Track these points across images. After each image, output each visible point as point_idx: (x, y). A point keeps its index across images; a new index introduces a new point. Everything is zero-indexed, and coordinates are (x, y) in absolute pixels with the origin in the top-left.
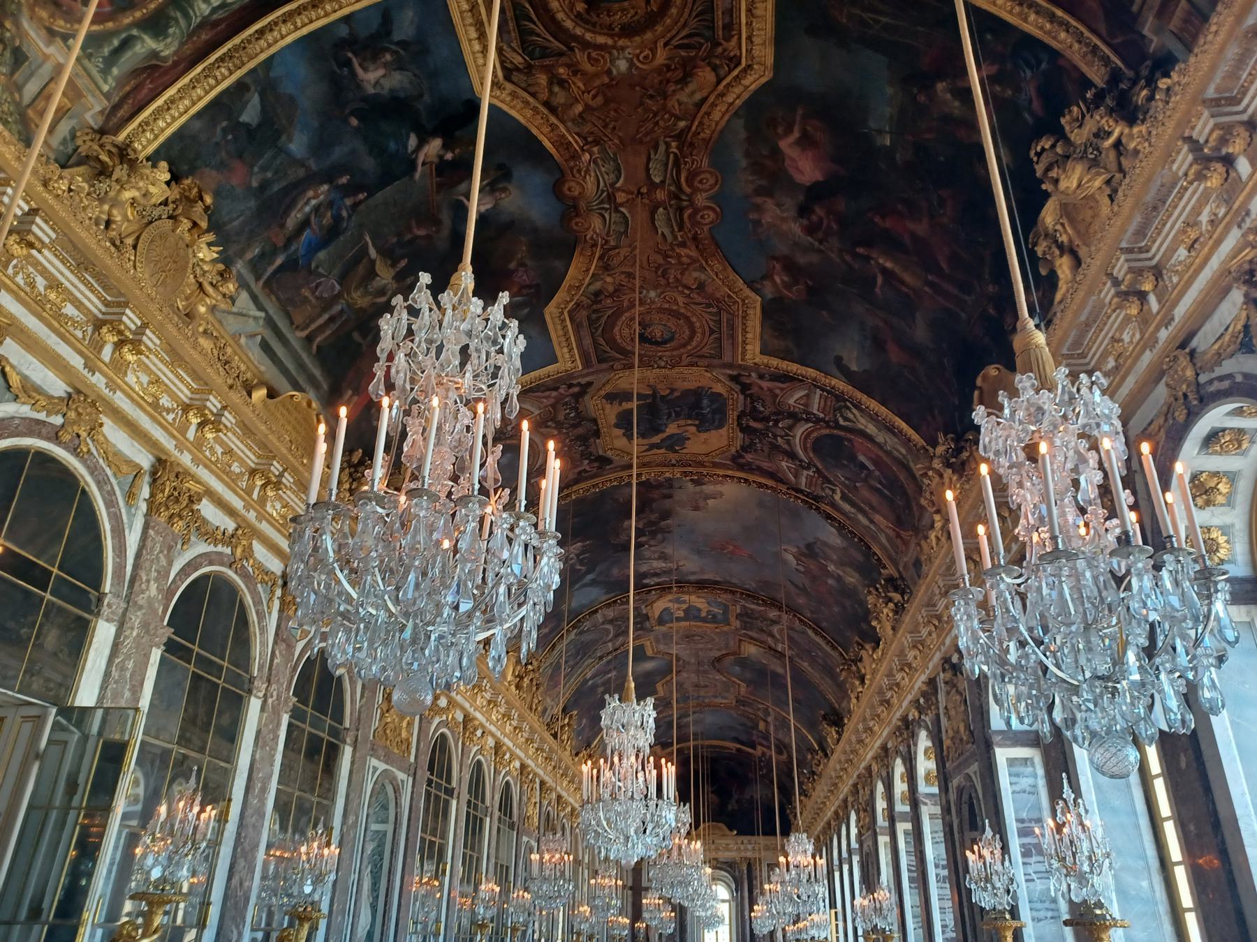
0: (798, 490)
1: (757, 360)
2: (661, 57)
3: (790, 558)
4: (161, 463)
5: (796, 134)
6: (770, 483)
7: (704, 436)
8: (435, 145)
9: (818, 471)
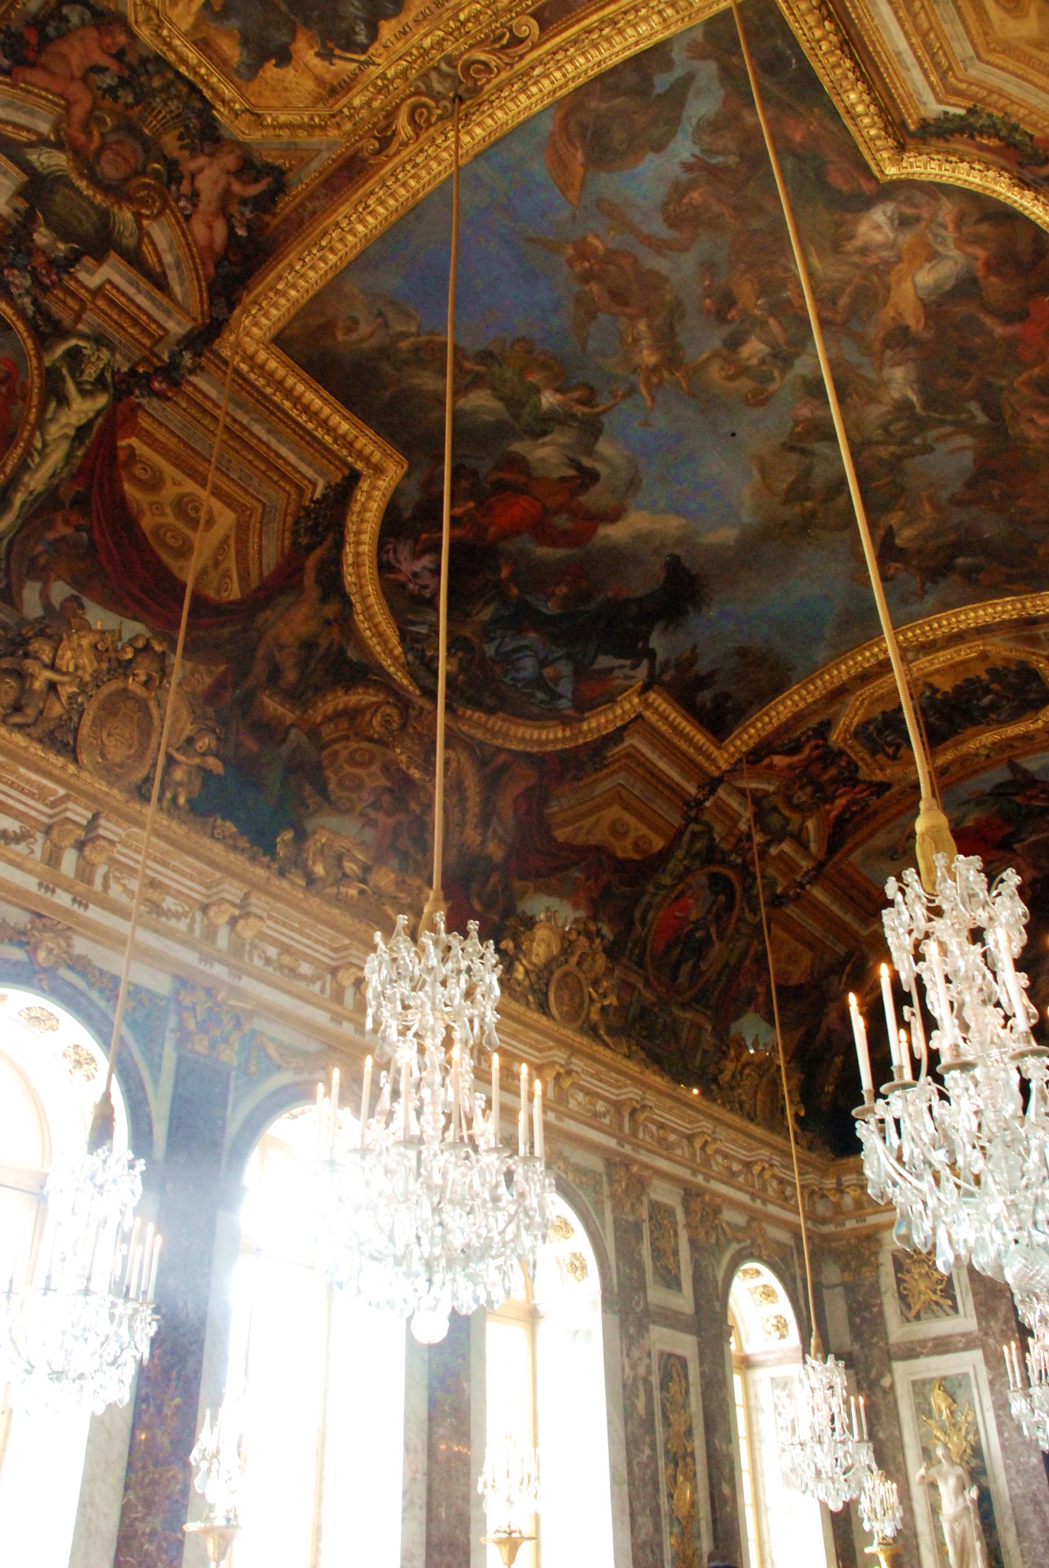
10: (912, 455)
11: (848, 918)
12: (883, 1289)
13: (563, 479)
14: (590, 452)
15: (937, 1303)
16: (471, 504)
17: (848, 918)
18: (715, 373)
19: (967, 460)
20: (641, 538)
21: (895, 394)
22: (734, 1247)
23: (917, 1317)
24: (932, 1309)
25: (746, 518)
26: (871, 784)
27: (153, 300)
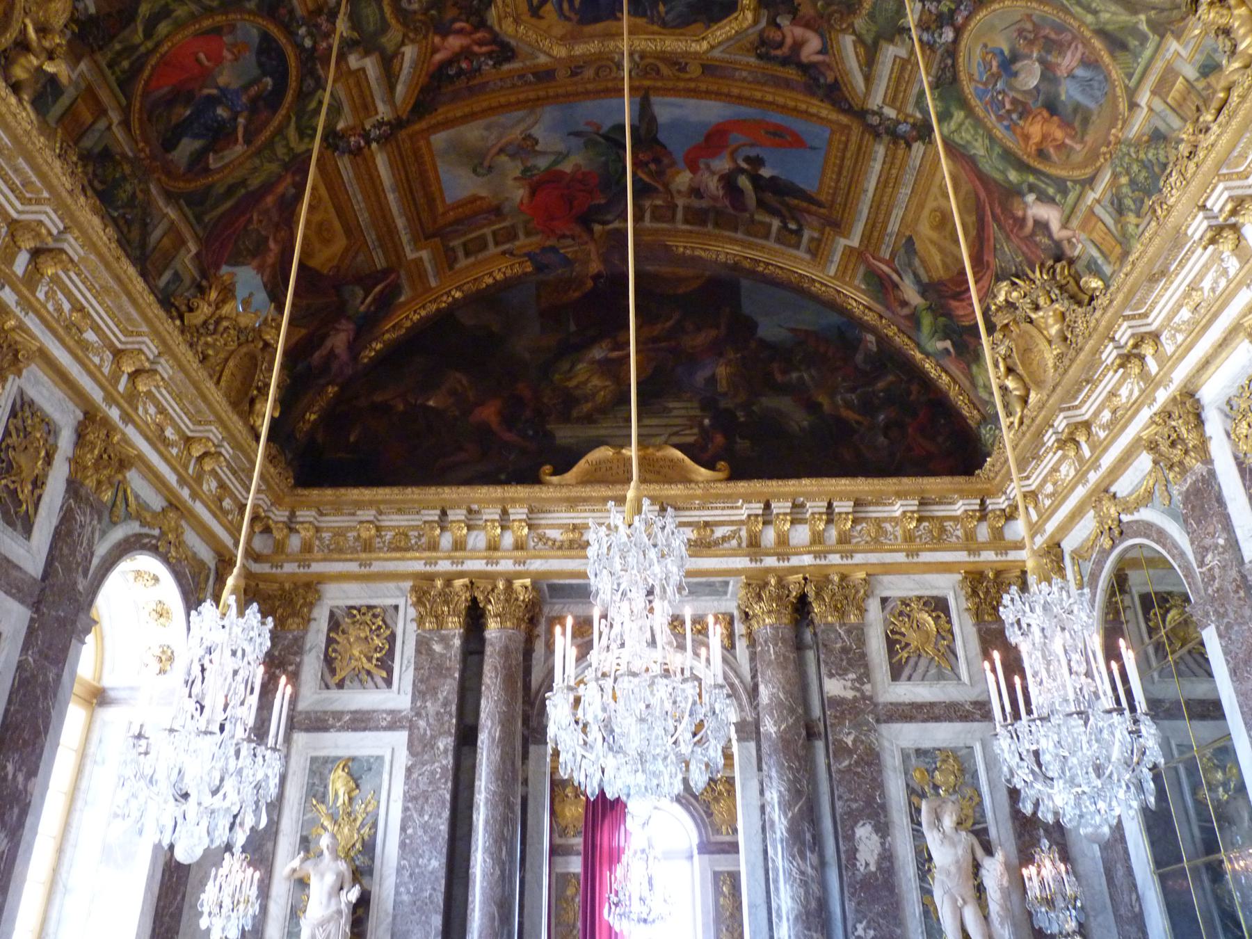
11: (400, 223)
12: (308, 646)
15: (369, 673)
17: (400, 223)
22: (134, 527)
23: (340, 685)
24: (361, 678)
26: (496, 39)
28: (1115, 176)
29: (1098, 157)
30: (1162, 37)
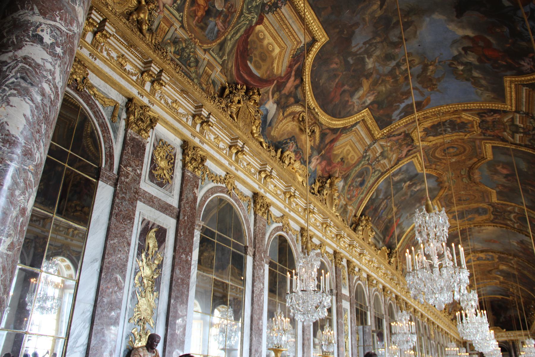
0: (514, 228)
1: (497, 202)
2: (464, 158)
3: (515, 244)
4: (369, 276)
5: (501, 166)
6: (504, 226)
7: (480, 217)
8: (408, 183)
9: (520, 224)
10: (370, 40)
13: (473, 52)
14: (460, 54)
16: (499, 62)
18: (417, 61)
19: (353, 44)
20: (463, 27)
21: (372, 60)
25: (428, 19)
27: (516, 118)
28: (185, 41)
29: (190, 32)
30: (221, 65)
